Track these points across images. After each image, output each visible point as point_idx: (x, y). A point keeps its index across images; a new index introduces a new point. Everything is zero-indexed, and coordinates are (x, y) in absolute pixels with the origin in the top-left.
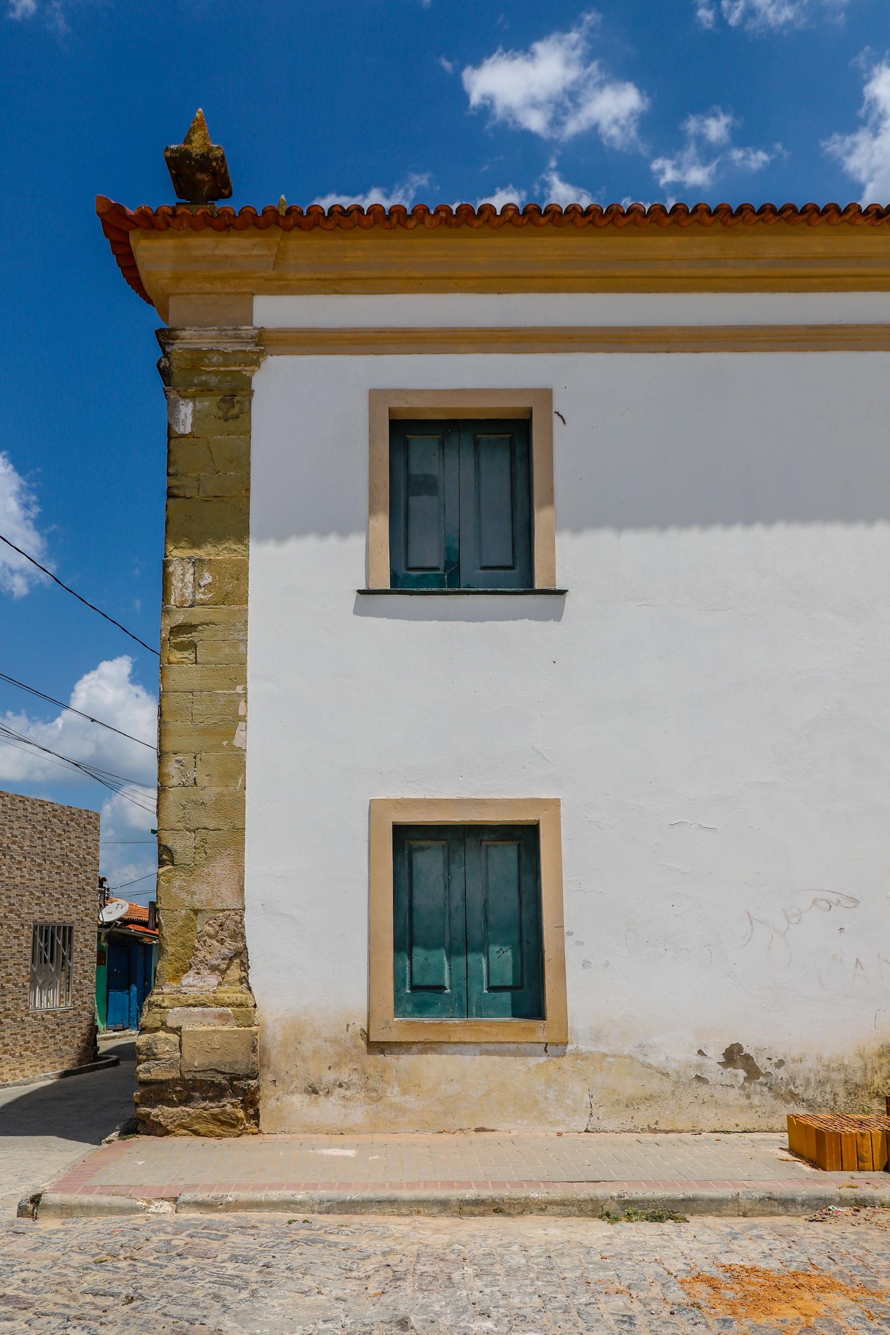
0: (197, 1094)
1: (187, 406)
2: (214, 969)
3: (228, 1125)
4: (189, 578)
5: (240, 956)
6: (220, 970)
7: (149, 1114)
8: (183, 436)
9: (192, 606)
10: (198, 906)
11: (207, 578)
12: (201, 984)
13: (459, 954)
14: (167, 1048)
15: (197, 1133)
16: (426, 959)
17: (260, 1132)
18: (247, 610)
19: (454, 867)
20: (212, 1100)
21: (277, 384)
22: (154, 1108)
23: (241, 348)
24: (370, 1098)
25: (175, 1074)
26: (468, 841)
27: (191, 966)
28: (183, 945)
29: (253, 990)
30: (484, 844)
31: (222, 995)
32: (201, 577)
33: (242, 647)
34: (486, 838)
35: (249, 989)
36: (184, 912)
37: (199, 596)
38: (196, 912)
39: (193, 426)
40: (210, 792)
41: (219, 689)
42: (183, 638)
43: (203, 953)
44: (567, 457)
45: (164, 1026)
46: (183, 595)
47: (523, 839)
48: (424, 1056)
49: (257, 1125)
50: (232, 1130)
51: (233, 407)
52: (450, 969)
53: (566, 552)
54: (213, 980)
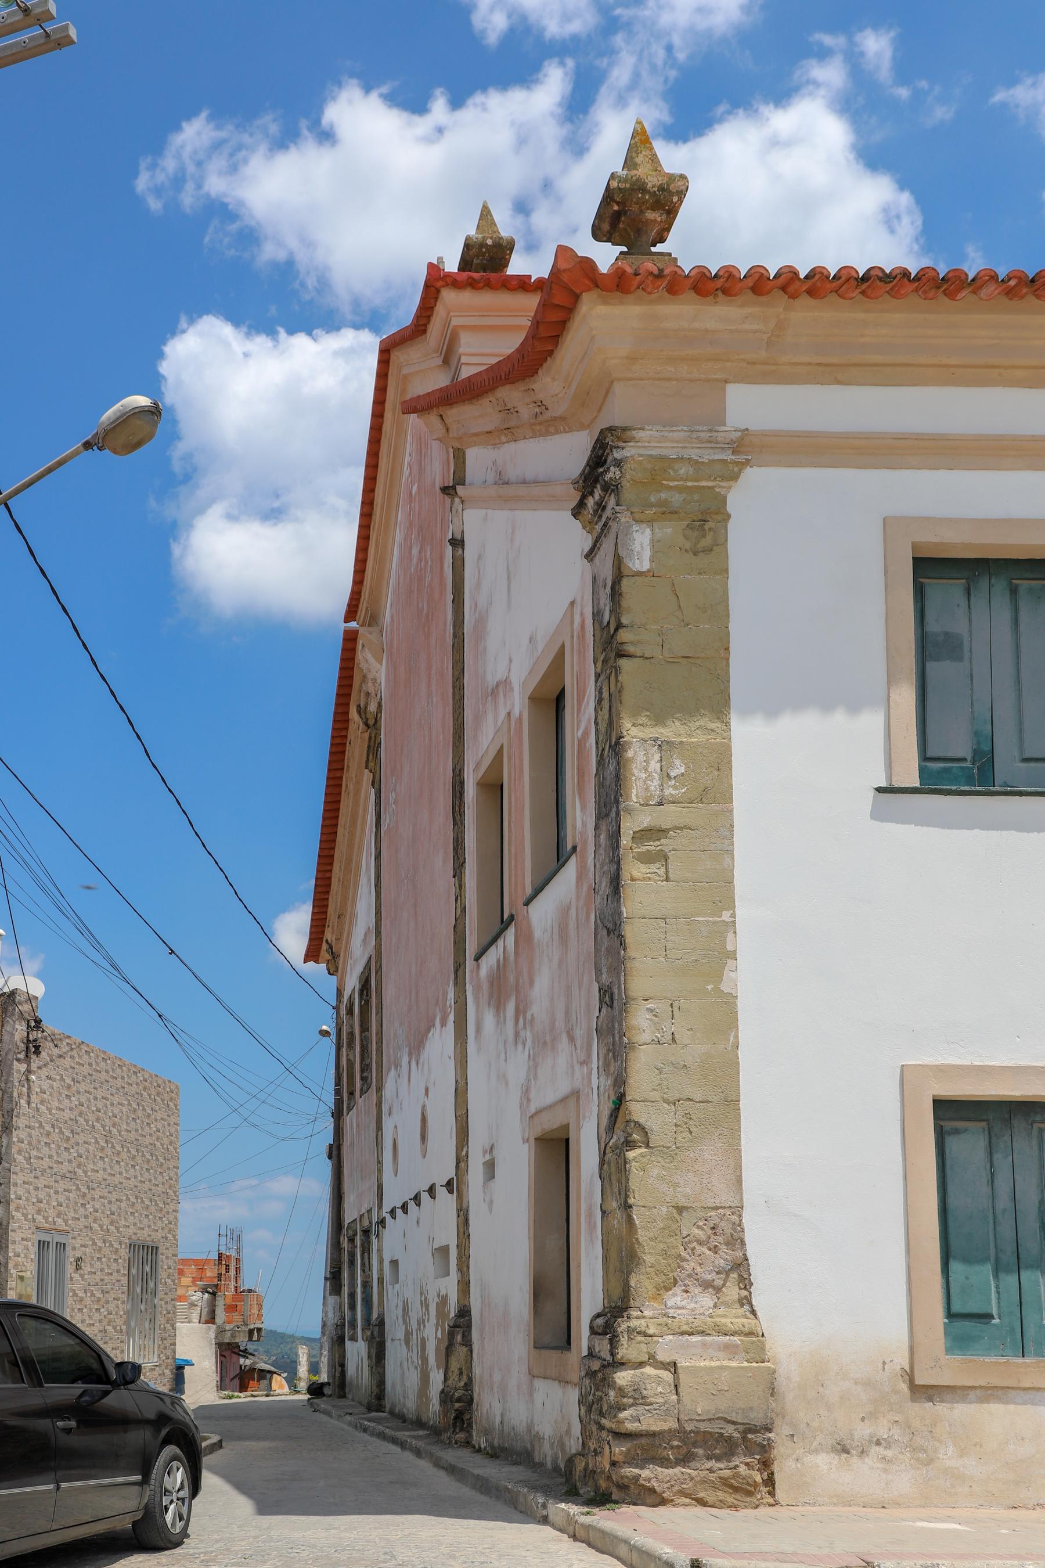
0: (700, 1451)
1: (643, 533)
2: (707, 1285)
3: (741, 1492)
4: (654, 766)
5: (740, 1269)
6: (714, 1287)
7: (637, 1478)
8: (640, 574)
9: (660, 804)
10: (683, 1202)
11: (679, 768)
12: (692, 1305)
13: (1008, 1271)
14: (660, 1389)
15: (702, 1503)
16: (967, 1278)
17: (777, 1503)
18: (732, 811)
19: (997, 1157)
20: (718, 1459)
22: (642, 1468)
23: (717, 457)
24: (918, 1459)
25: (672, 1424)
26: (1015, 1123)
27: (675, 1282)
28: (665, 1254)
29: (759, 1314)
30: (1035, 1126)
31: (723, 1320)
32: (671, 765)
33: (728, 860)
34: (1038, 1118)
35: (753, 1312)
36: (664, 1209)
37: (669, 791)
38: (680, 1210)
39: (652, 561)
41: (699, 915)
42: (652, 846)
43: (692, 1264)
45: (652, 1360)
46: (647, 789)
48: (985, 1405)
49: (772, 1493)
50: (748, 1499)
51: (704, 536)
52: (998, 1293)
54: (706, 1300)
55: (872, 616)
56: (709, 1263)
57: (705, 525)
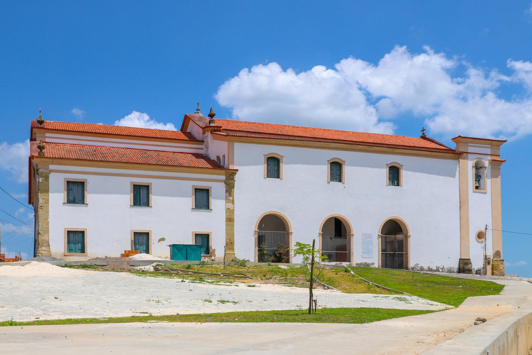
5: (49, 245)
21: (52, 176)
40: (45, 226)
44: (89, 187)
47: (83, 233)
53: (89, 197)
54: (45, 248)
55: (63, 186)
56: (46, 245)
57: (47, 178)
